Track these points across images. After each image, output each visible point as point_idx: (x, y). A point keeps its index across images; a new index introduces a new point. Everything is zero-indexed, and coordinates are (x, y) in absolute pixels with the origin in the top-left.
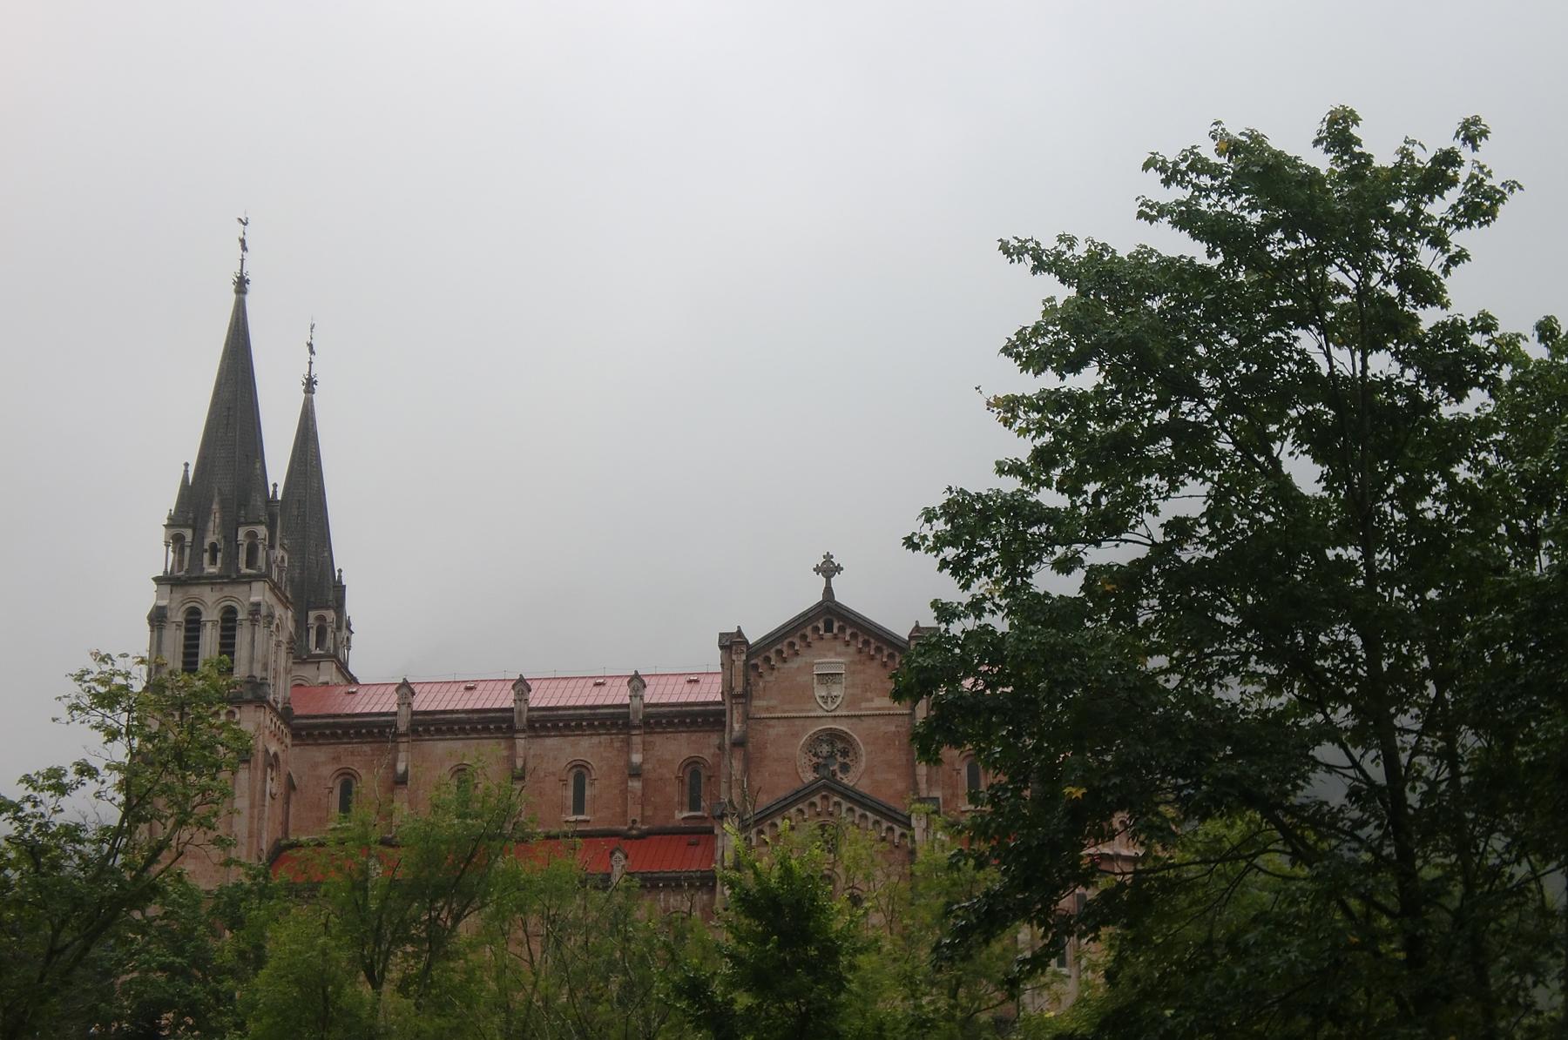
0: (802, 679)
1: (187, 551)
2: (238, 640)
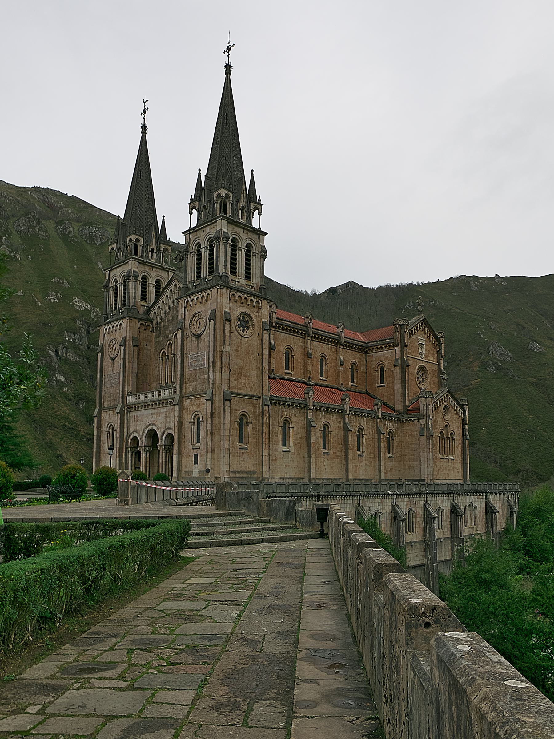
0: (416, 344)
1: (229, 206)
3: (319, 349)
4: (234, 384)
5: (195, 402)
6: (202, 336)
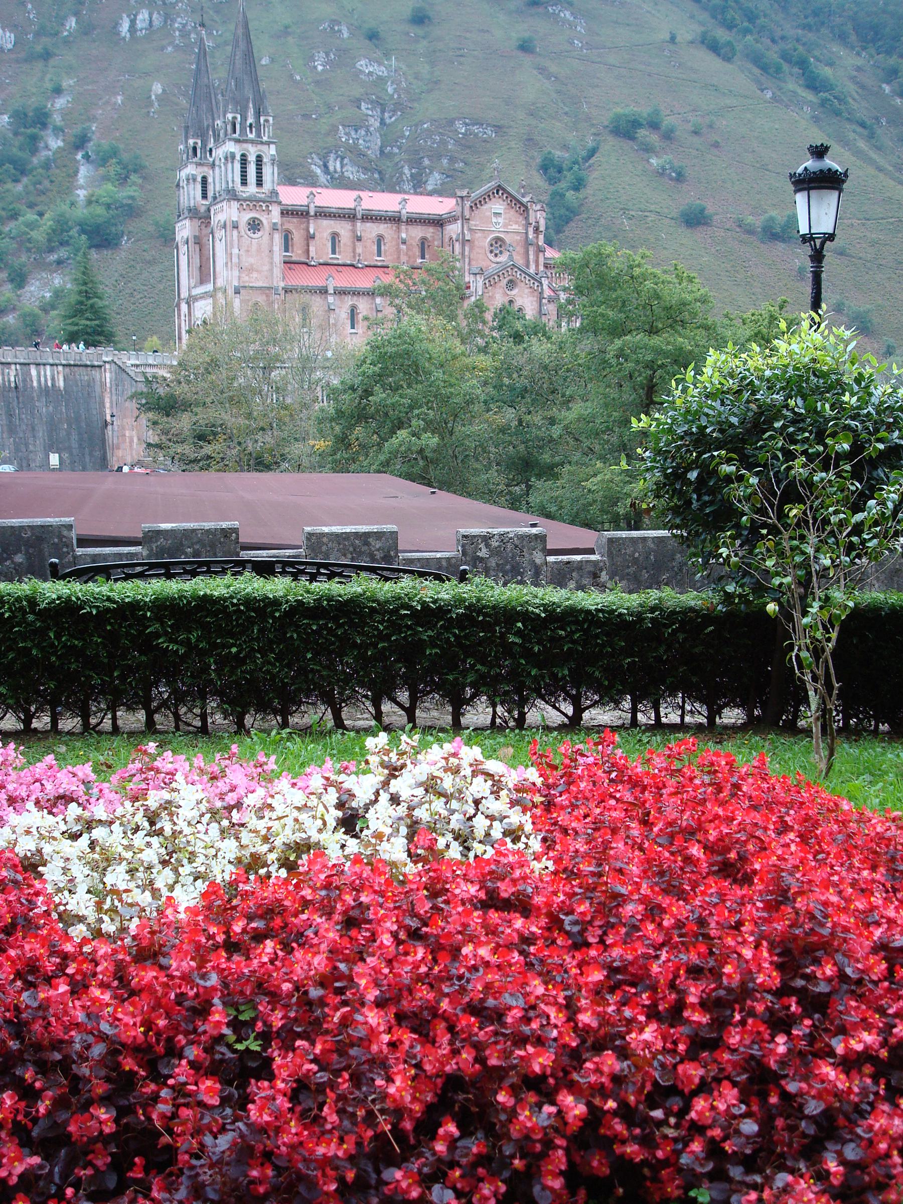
0: (488, 214)
1: (238, 126)
2: (264, 171)
3: (371, 230)
4: (247, 278)
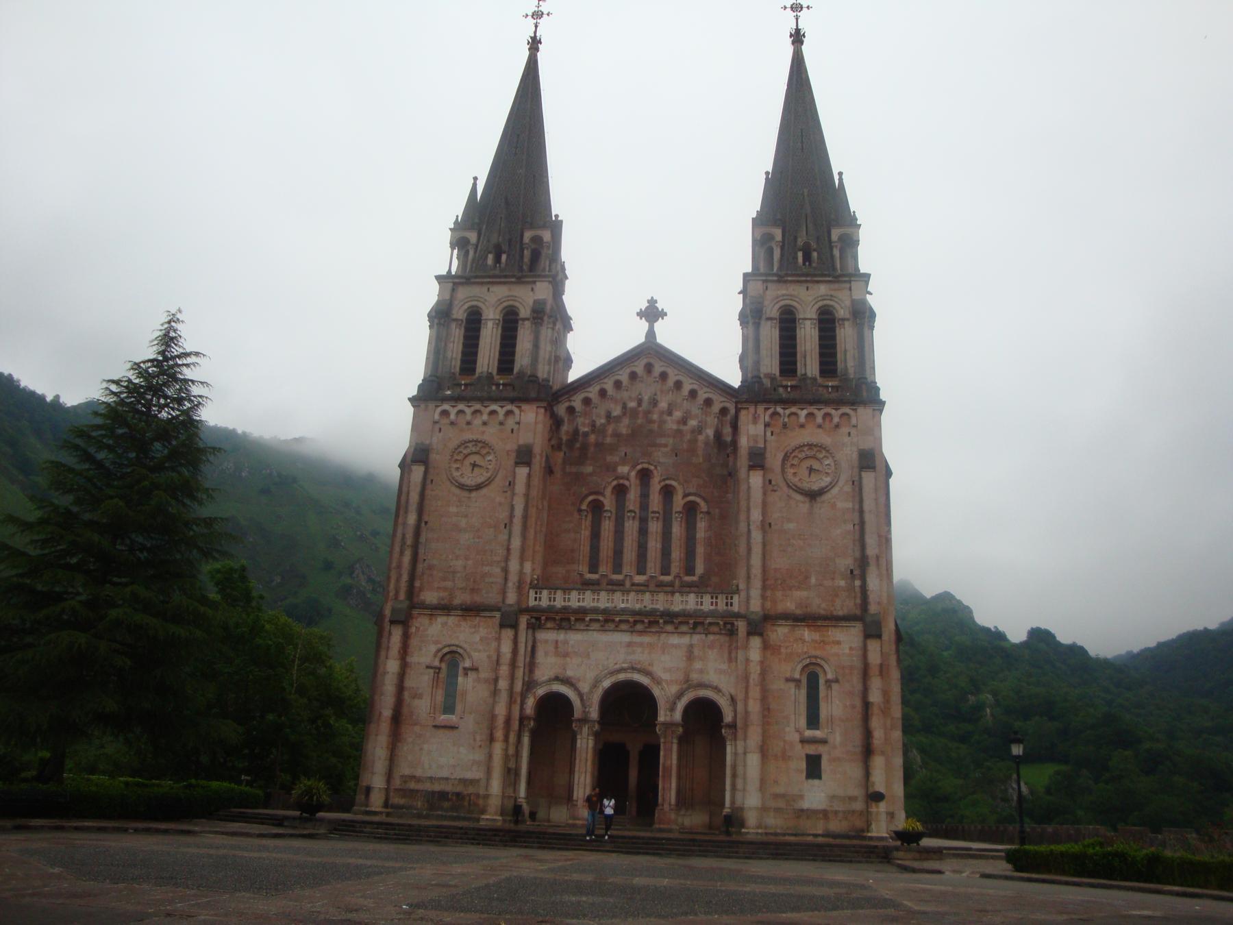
5: (807, 634)
6: (826, 497)
